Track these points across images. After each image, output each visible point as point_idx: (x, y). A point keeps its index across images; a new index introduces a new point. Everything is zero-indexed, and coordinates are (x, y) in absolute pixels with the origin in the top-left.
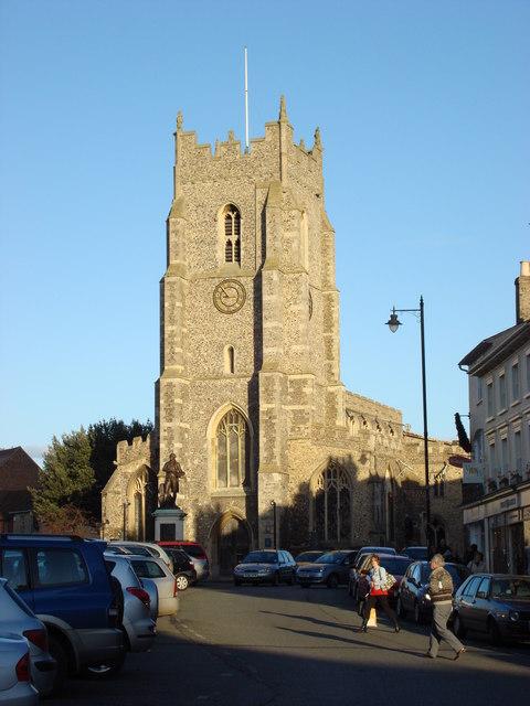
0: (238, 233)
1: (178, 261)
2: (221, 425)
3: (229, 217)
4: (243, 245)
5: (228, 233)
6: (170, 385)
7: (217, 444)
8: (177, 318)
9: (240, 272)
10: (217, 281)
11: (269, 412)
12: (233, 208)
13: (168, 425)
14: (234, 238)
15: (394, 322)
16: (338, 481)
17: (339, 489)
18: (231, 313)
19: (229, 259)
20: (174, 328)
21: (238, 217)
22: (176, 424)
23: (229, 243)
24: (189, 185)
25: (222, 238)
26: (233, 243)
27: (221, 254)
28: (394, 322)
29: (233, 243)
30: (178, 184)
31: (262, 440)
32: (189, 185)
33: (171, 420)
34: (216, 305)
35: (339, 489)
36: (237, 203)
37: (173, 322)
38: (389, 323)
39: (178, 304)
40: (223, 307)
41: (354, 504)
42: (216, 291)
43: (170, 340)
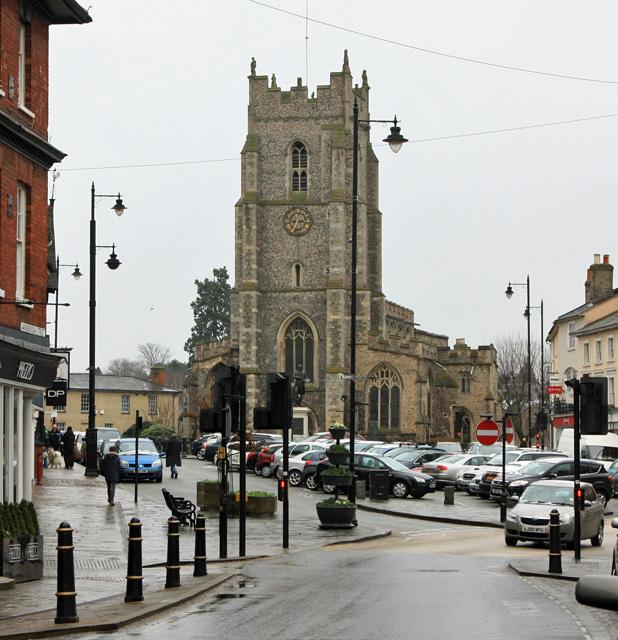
0: (304, 165)
2: (288, 331)
3: (295, 152)
4: (309, 177)
5: (295, 165)
6: (249, 297)
7: (284, 346)
11: (335, 322)
12: (298, 144)
13: (248, 330)
14: (299, 170)
15: (509, 292)
16: (390, 380)
17: (390, 387)
18: (299, 236)
19: (295, 188)
21: (304, 151)
23: (296, 174)
25: (289, 169)
27: (288, 185)
28: (509, 292)
33: (249, 326)
34: (287, 230)
35: (390, 387)
36: (301, 138)
41: (404, 399)
42: (286, 217)
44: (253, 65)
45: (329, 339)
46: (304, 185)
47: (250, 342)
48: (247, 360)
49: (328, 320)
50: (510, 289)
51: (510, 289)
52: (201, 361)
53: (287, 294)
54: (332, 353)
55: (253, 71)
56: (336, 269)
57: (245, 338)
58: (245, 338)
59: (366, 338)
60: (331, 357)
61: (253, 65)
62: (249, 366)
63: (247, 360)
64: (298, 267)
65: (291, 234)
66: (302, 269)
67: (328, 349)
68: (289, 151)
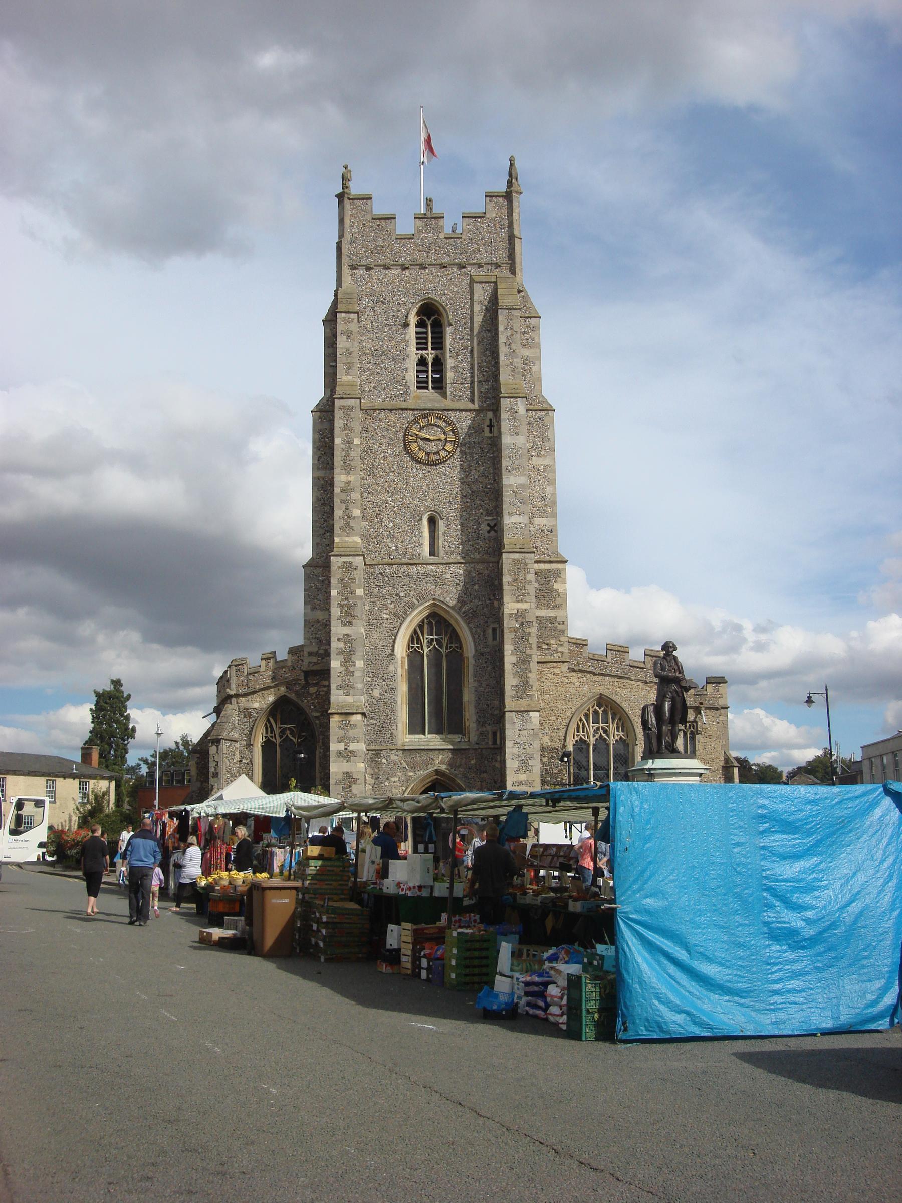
0: (439, 344)
1: (350, 378)
3: (421, 324)
5: (421, 344)
6: (349, 567)
8: (357, 462)
9: (448, 404)
10: (410, 415)
11: (520, 615)
14: (430, 355)
15: (809, 701)
18: (435, 464)
19: (422, 385)
20: (351, 478)
22: (359, 629)
23: (422, 362)
24: (362, 271)
25: (413, 355)
26: (430, 360)
27: (412, 376)
28: (809, 701)
29: (430, 360)
30: (346, 270)
31: (509, 659)
32: (362, 271)
33: (350, 623)
34: (408, 451)
37: (348, 468)
38: (807, 702)
39: (357, 441)
40: (422, 455)
43: (344, 496)
44: (345, 179)
45: (508, 648)
46: (439, 385)
47: (352, 652)
48: (347, 687)
49: (507, 611)
50: (809, 698)
51: (809, 698)
52: (245, 695)
53: (415, 569)
54: (514, 674)
55: (345, 187)
56: (514, 519)
57: (341, 645)
58: (341, 645)
59: (565, 649)
60: (514, 682)
61: (345, 179)
62: (350, 699)
63: (347, 687)
64: (432, 521)
65: (418, 461)
66: (442, 525)
67: (508, 666)
68: (413, 320)
